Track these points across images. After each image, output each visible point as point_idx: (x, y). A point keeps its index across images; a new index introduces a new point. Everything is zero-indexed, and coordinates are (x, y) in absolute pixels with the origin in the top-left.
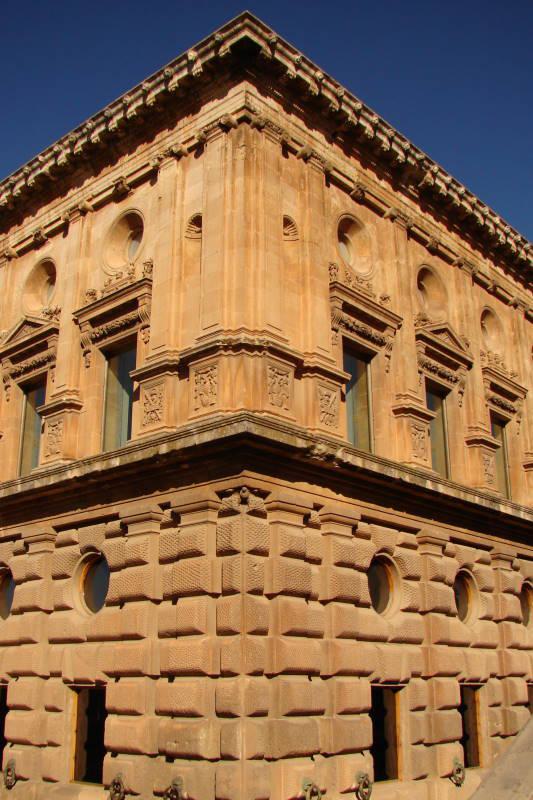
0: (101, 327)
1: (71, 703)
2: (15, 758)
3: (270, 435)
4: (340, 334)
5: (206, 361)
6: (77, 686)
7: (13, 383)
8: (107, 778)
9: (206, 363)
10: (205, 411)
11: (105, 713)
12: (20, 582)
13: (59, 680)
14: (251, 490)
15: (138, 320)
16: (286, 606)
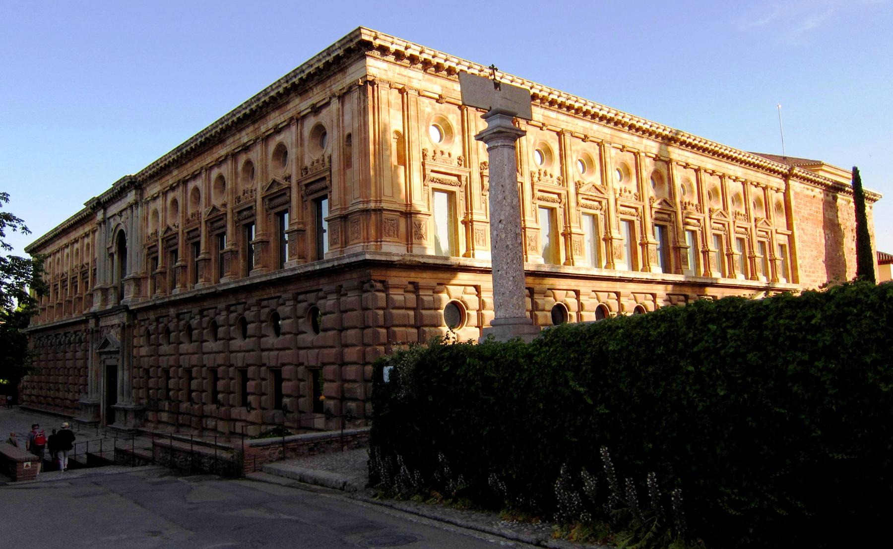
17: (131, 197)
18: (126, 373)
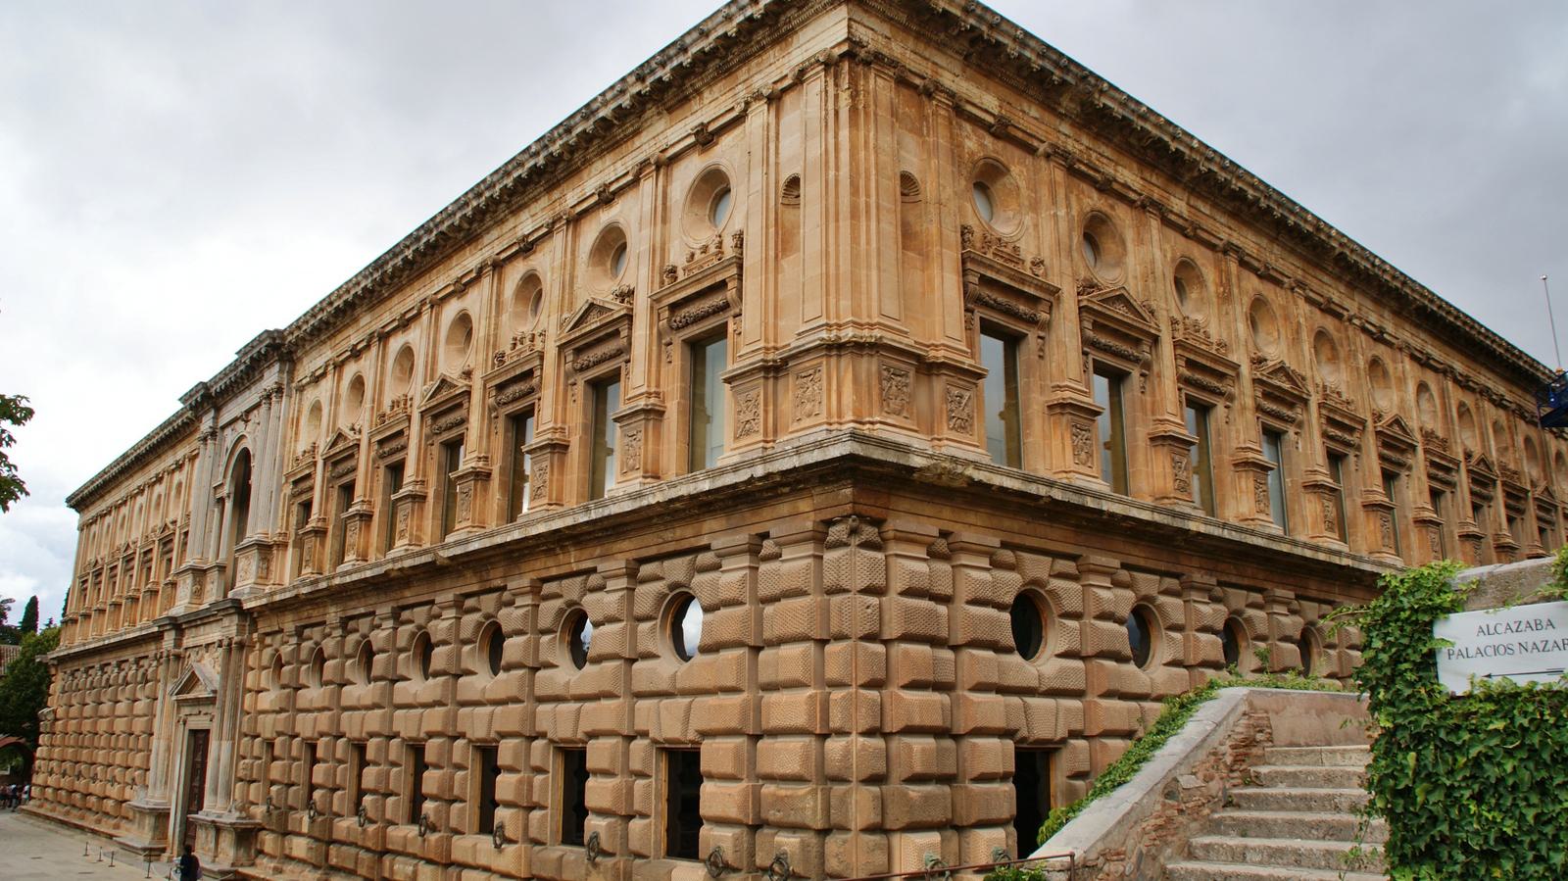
4: (977, 315)
9: (807, 365)
14: (861, 517)
15: (726, 307)
17: (271, 377)
18: (226, 745)
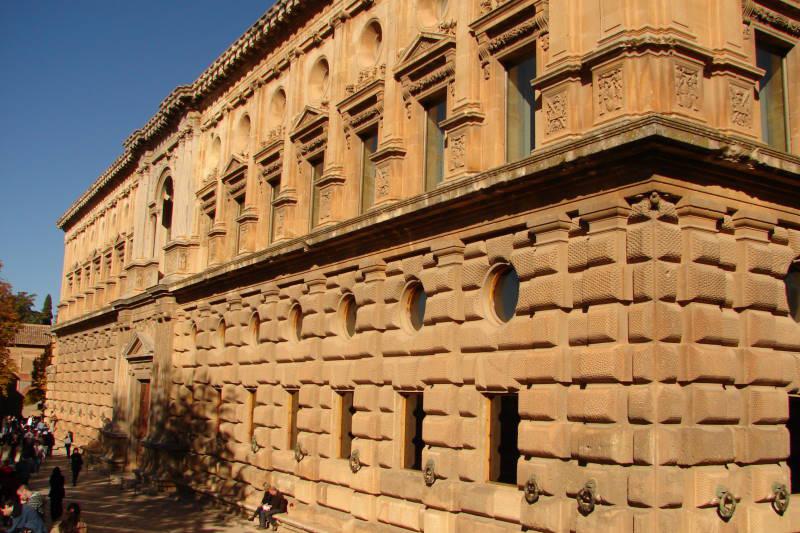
0: (498, 38)
1: (484, 409)
2: (434, 459)
3: (681, 137)
4: (752, 28)
5: (609, 64)
6: (490, 393)
7: (413, 100)
8: (521, 479)
10: (610, 116)
11: (518, 418)
12: (431, 294)
13: (472, 388)
14: (662, 195)
15: (536, 27)
16: (700, 313)
